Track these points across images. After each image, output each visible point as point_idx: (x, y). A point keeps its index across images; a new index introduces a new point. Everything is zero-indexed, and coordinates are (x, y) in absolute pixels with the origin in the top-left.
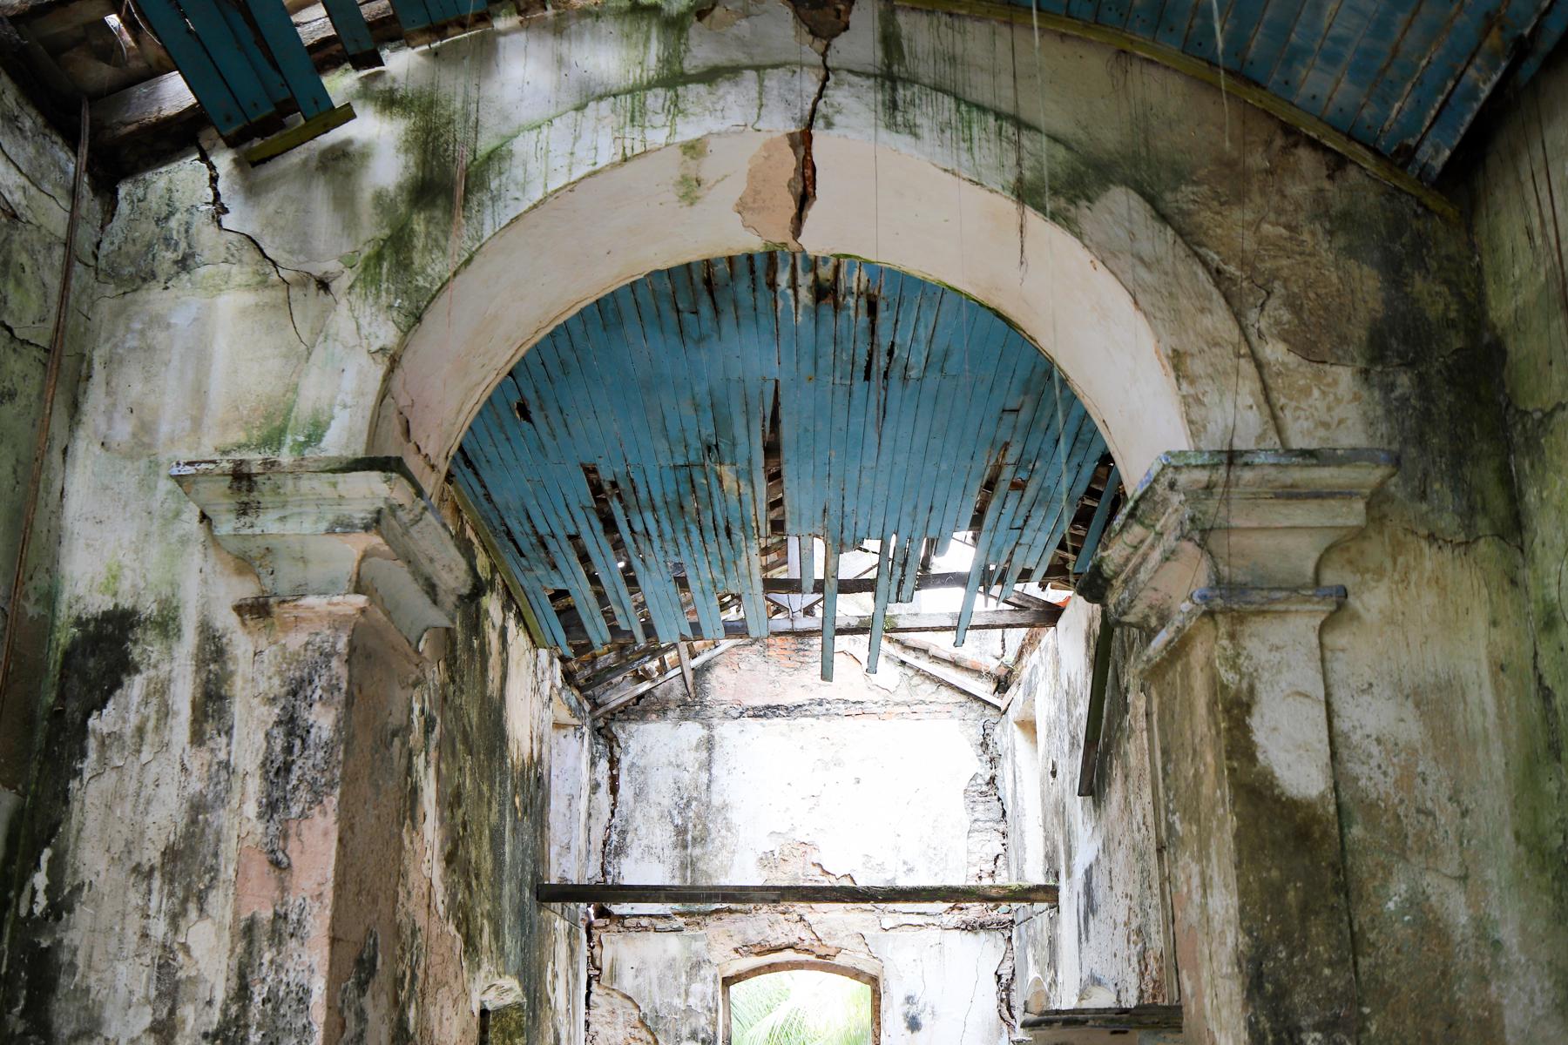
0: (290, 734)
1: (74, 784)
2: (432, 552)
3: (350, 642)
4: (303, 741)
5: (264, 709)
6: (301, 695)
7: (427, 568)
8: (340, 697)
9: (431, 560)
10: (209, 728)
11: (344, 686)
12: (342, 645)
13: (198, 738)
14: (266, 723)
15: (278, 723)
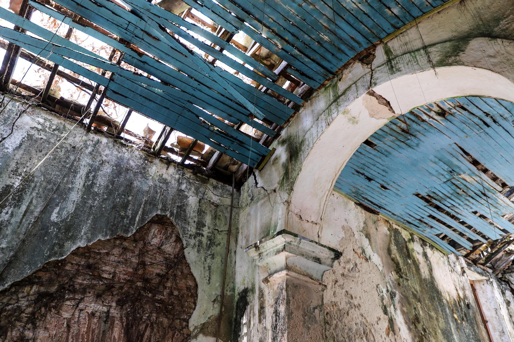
0: (276, 315)
1: (239, 339)
2: (311, 249)
3: (286, 284)
4: (279, 317)
5: (271, 309)
6: (277, 304)
7: (314, 255)
8: (285, 301)
9: (313, 252)
10: (262, 317)
11: (286, 298)
12: (285, 286)
13: (260, 321)
14: (271, 313)
15: (274, 313)
